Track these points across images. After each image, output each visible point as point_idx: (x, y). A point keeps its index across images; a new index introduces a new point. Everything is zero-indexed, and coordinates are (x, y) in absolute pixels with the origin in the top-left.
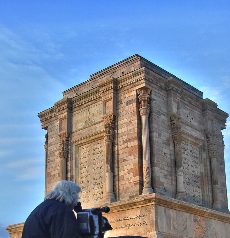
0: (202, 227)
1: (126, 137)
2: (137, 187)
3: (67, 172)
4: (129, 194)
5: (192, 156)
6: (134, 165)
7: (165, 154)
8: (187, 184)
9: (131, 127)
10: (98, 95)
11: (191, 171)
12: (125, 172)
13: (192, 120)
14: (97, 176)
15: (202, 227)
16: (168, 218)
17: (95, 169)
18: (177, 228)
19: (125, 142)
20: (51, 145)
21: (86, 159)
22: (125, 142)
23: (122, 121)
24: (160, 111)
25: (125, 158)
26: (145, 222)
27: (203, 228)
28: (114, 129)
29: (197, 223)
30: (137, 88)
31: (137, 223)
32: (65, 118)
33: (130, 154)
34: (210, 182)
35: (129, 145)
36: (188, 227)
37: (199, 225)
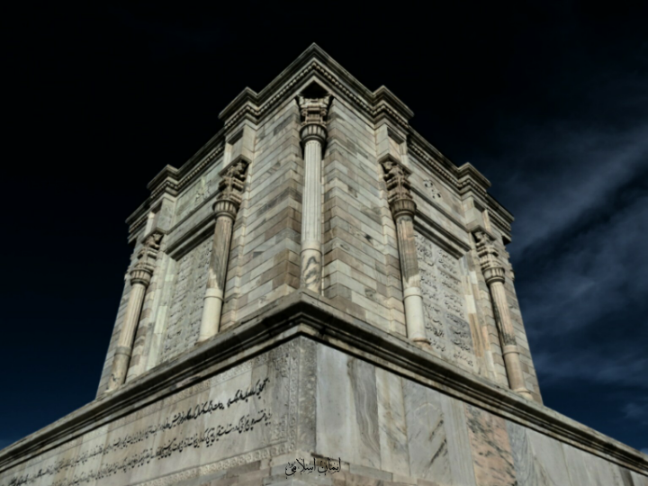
0: (498, 449)
1: (265, 201)
5: (443, 273)
7: (368, 237)
8: (436, 333)
11: (445, 307)
12: (253, 283)
13: (436, 196)
15: (498, 449)
16: (368, 403)
18: (407, 446)
19: (261, 212)
24: (357, 146)
25: (257, 250)
26: (262, 414)
27: (503, 454)
29: (480, 434)
31: (236, 423)
34: (496, 340)
36: (448, 446)
37: (490, 443)
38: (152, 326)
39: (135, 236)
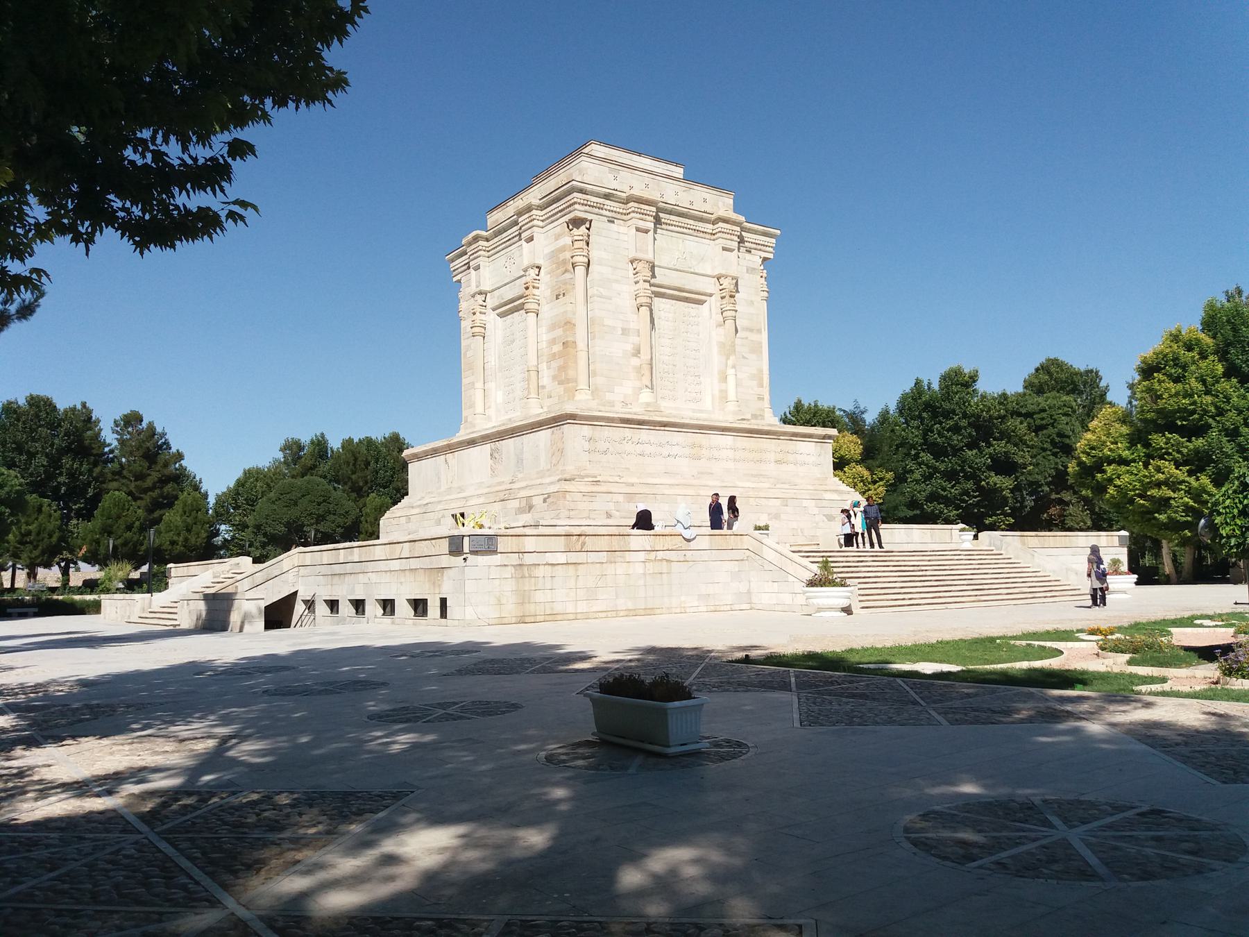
32: (646, 231)
39: (589, 217)
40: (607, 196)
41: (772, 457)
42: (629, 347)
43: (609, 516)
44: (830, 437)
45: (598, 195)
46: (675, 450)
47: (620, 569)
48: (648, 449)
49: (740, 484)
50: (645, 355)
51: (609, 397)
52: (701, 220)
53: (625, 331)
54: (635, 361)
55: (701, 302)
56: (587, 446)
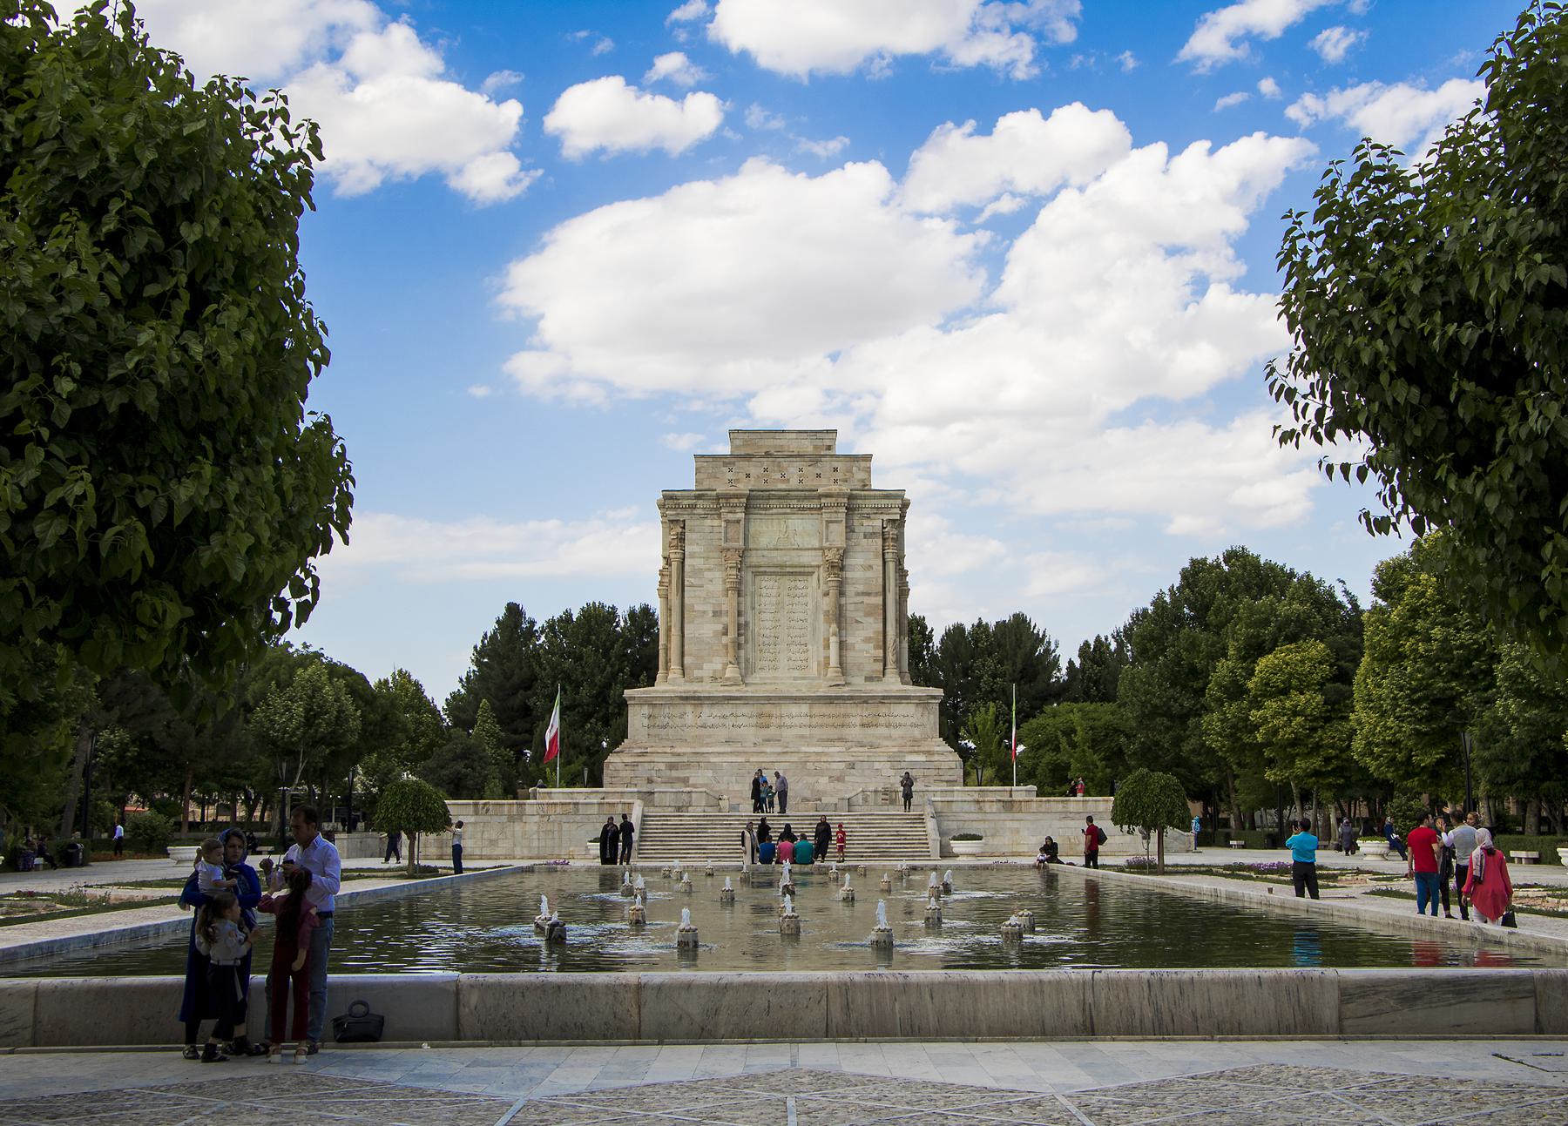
1: (861, 588)
2: (880, 666)
3: (739, 614)
4: (865, 673)
6: (876, 632)
9: (869, 574)
10: (806, 504)
14: (797, 632)
17: (791, 620)
19: (858, 594)
20: (693, 556)
21: (774, 600)
22: (858, 594)
23: (856, 560)
28: (842, 569)
30: (886, 517)
32: (738, 521)
33: (868, 614)
35: (867, 600)
38: (747, 624)
40: (698, 497)
41: (858, 720)
42: (720, 627)
43: (650, 781)
44: (934, 697)
45: (688, 498)
46: (741, 720)
47: (518, 827)
48: (711, 721)
49: (804, 749)
50: (732, 634)
51: (697, 673)
52: (806, 498)
53: (716, 614)
54: (725, 640)
55: (811, 574)
56: (646, 722)
